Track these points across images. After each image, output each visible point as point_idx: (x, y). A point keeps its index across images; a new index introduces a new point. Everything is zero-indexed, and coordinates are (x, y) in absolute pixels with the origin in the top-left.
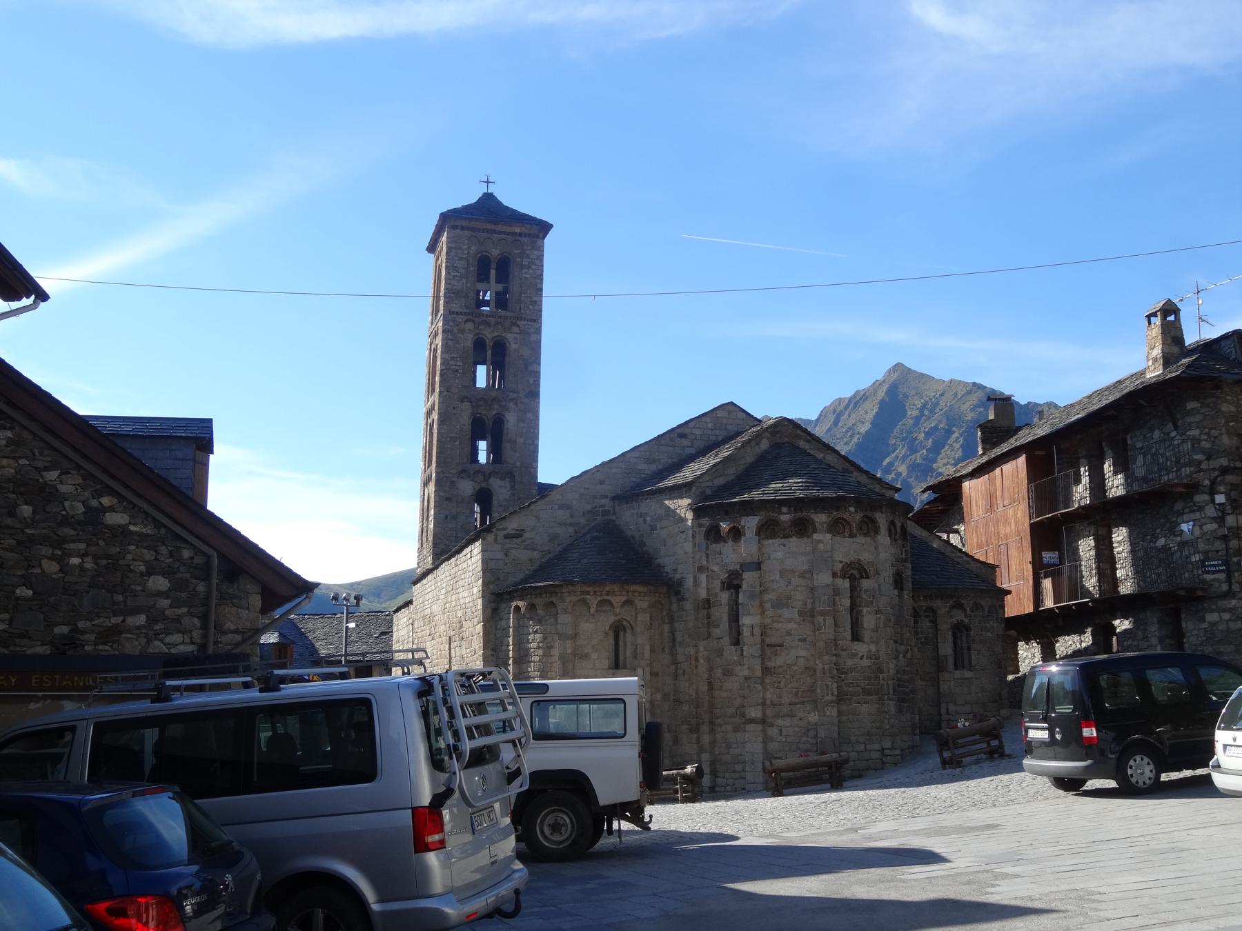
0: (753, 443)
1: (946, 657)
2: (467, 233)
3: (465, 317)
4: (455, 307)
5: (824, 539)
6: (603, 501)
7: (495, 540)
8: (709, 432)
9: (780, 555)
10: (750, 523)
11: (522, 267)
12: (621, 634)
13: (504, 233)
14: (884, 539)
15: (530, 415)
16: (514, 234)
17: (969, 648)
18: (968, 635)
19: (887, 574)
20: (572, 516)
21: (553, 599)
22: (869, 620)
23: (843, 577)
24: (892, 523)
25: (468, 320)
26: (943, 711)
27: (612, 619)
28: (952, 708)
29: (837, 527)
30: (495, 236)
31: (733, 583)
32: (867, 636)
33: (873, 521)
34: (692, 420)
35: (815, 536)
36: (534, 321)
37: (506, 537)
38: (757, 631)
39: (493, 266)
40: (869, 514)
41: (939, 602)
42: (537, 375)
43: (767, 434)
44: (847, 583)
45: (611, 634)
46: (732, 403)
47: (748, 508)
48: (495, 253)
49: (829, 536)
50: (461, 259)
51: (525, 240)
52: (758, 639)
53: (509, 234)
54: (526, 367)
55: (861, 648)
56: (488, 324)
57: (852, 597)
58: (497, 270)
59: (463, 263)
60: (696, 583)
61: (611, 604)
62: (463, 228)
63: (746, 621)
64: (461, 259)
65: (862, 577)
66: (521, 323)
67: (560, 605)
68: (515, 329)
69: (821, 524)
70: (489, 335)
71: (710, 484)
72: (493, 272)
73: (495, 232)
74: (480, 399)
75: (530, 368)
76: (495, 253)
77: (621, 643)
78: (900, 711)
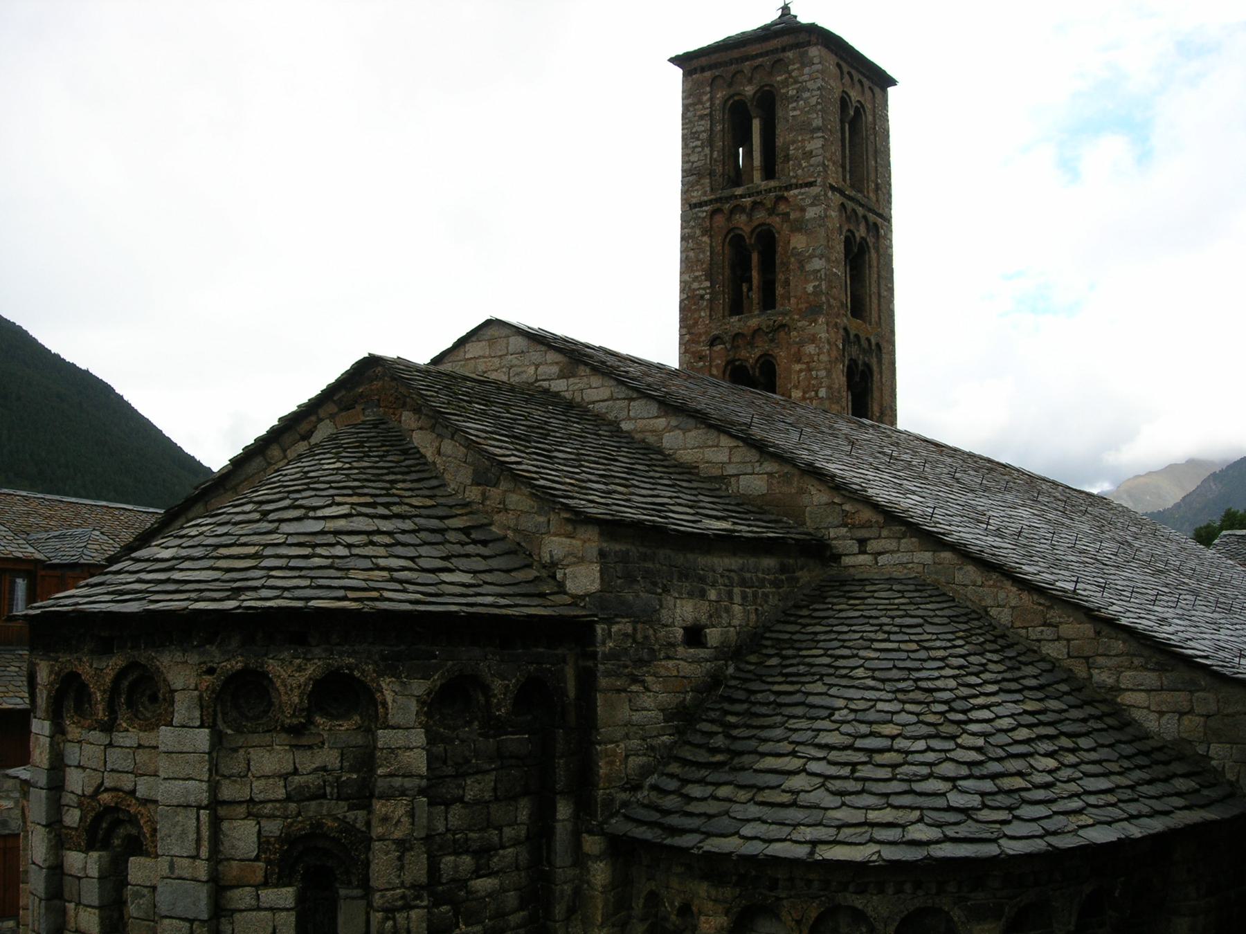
4: (697, 196)
14: (184, 738)
16: (775, 51)
36: (811, 184)
50: (702, 117)
51: (790, 54)
53: (767, 53)
56: (742, 209)
59: (706, 124)
62: (703, 70)
64: (702, 117)
68: (782, 207)
74: (737, 335)
75: (808, 267)
76: (749, 90)
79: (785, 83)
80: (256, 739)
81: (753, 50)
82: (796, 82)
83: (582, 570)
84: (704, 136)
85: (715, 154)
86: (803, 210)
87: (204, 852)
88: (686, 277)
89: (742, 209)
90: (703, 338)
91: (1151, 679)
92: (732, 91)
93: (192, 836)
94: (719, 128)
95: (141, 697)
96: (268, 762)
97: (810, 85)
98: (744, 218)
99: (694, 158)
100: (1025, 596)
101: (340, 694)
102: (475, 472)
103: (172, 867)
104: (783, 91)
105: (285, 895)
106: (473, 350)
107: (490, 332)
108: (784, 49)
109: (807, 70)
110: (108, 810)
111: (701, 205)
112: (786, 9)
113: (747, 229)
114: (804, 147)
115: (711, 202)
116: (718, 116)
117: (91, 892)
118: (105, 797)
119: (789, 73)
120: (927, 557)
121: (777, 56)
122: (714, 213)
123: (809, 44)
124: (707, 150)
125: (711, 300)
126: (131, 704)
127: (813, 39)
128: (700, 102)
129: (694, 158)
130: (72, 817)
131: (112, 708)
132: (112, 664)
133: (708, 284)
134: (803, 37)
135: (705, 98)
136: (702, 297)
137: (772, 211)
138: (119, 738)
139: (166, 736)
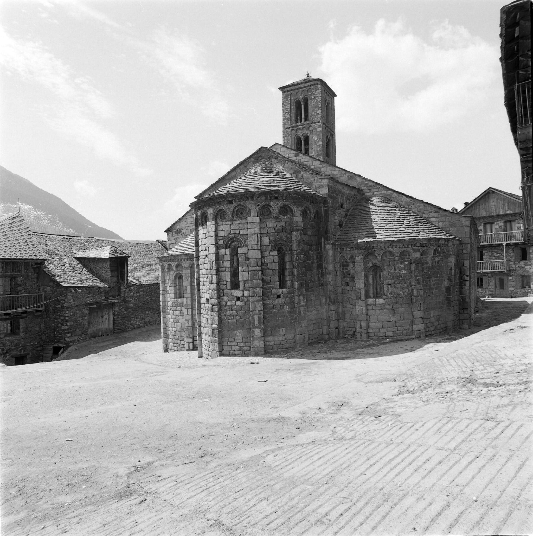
2: (289, 93)
7: (172, 235)
14: (254, 219)
16: (308, 86)
22: (243, 276)
27: (176, 273)
29: (219, 216)
33: (243, 207)
36: (318, 122)
40: (241, 203)
41: (356, 251)
44: (228, 251)
46: (276, 144)
51: (312, 87)
53: (306, 87)
55: (237, 293)
56: (300, 129)
57: (232, 261)
59: (289, 106)
68: (311, 128)
70: (300, 134)
72: (303, 106)
73: (300, 88)
79: (311, 95)
80: (268, 220)
81: (301, 86)
83: (323, 189)
84: (289, 109)
86: (316, 129)
87: (259, 243)
89: (300, 129)
91: (436, 215)
92: (296, 97)
93: (256, 240)
94: (292, 107)
95: (241, 213)
96: (271, 224)
97: (318, 95)
98: (300, 131)
99: (286, 115)
100: (408, 199)
101: (285, 210)
102: (294, 171)
103: (252, 247)
105: (276, 253)
108: (311, 86)
110: (232, 238)
111: (288, 128)
116: (292, 104)
117: (227, 258)
120: (385, 192)
122: (292, 130)
126: (237, 215)
127: (319, 83)
128: (287, 100)
130: (221, 242)
131: (233, 216)
134: (316, 82)
138: (235, 222)
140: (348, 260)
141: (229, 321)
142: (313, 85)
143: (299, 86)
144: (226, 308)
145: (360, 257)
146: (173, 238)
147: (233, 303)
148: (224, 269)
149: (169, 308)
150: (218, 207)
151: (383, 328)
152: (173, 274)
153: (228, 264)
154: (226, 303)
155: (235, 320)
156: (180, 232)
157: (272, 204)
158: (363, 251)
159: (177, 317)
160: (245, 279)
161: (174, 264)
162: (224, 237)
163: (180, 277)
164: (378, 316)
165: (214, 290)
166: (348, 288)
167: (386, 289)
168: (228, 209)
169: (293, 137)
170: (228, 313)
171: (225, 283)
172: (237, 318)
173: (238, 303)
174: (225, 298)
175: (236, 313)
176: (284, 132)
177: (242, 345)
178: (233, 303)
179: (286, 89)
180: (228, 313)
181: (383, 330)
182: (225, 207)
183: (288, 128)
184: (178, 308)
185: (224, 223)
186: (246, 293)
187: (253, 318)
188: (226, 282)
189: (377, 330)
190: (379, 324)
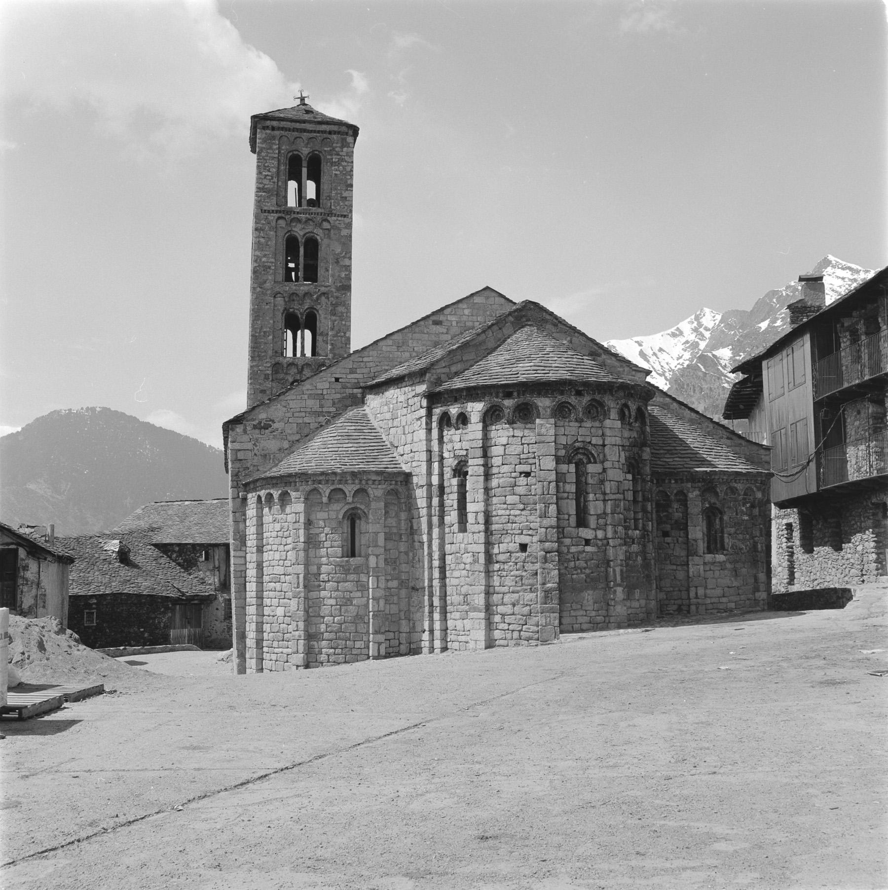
0: (495, 328)
1: (695, 540)
2: (277, 133)
3: (276, 215)
5: (545, 426)
6: (355, 391)
7: (245, 431)
8: (465, 318)
9: (504, 441)
10: (475, 409)
11: (333, 164)
12: (358, 521)
13: (315, 132)
14: (613, 423)
15: (340, 309)
16: (324, 132)
17: (722, 532)
18: (721, 519)
19: (615, 456)
20: (322, 406)
21: (286, 489)
22: (595, 506)
23: (570, 462)
24: (626, 405)
25: (279, 218)
26: (692, 594)
27: (347, 507)
28: (701, 591)
29: (561, 412)
30: (305, 135)
31: (460, 471)
32: (592, 522)
33: (601, 404)
34: (447, 307)
35: (538, 421)
36: (345, 216)
37: (255, 427)
38: (481, 518)
39: (305, 164)
41: (689, 485)
42: (348, 268)
43: (511, 319)
44: (572, 468)
45: (346, 526)
46: (487, 288)
47: (472, 393)
48: (305, 151)
49: (552, 421)
51: (335, 137)
52: (482, 527)
53: (319, 132)
54: (337, 262)
56: (299, 221)
57: (578, 482)
58: (308, 168)
60: (429, 473)
61: (344, 493)
62: (273, 129)
63: (470, 507)
65: (590, 462)
66: (332, 219)
67: (293, 494)
69: (544, 409)
70: (299, 231)
71: (446, 370)
72: (304, 171)
73: (305, 131)
74: (293, 294)
75: (341, 263)
76: (305, 151)
77: (357, 530)
78: (629, 596)
82: (338, 155)
85: (280, 183)
88: (258, 253)
89: (299, 221)
90: (269, 292)
92: (294, 147)
94: (282, 168)
95: (596, 411)
98: (300, 226)
99: (266, 182)
104: (329, 157)
106: (477, 300)
107: (487, 293)
108: (330, 133)
109: (345, 149)
110: (579, 448)
112: (302, 99)
113: (302, 233)
114: (341, 194)
115: (277, 212)
116: (282, 159)
118: (577, 444)
119: (334, 149)
120: (661, 400)
121: (325, 135)
122: (279, 218)
123: (347, 134)
124: (275, 180)
125: (275, 269)
128: (271, 148)
129: (266, 182)
132: (586, 399)
133: (273, 260)
134: (344, 129)
135: (275, 147)
136: (269, 267)
137: (320, 225)
138: (584, 424)
139: (607, 423)
140: (673, 497)
141: (574, 576)
142: (335, 133)
143: (303, 126)
144: (569, 556)
145: (694, 493)
146: (246, 438)
147: (580, 548)
148: (565, 495)
149: (323, 577)
150: (563, 398)
151: (724, 596)
152: (339, 510)
153: (572, 488)
154: (569, 549)
155: (583, 576)
156: (267, 427)
157: (629, 403)
158: (700, 484)
159: (347, 595)
160: (599, 512)
161: (349, 489)
162: (565, 447)
163: (353, 518)
164: (716, 579)
165: (552, 527)
166: (668, 539)
167: (726, 540)
168: (580, 403)
169: (281, 233)
170: (572, 564)
171: (566, 517)
172: (587, 571)
173: (588, 549)
174: (567, 541)
175: (585, 565)
176: (257, 217)
177: (594, 614)
178: (580, 548)
179: (268, 123)
180: (572, 564)
181: (724, 600)
182: (573, 400)
183: (269, 212)
184: (352, 577)
185: (566, 424)
186: (600, 534)
187: (614, 571)
188: (569, 515)
189: (716, 600)
190: (719, 592)
